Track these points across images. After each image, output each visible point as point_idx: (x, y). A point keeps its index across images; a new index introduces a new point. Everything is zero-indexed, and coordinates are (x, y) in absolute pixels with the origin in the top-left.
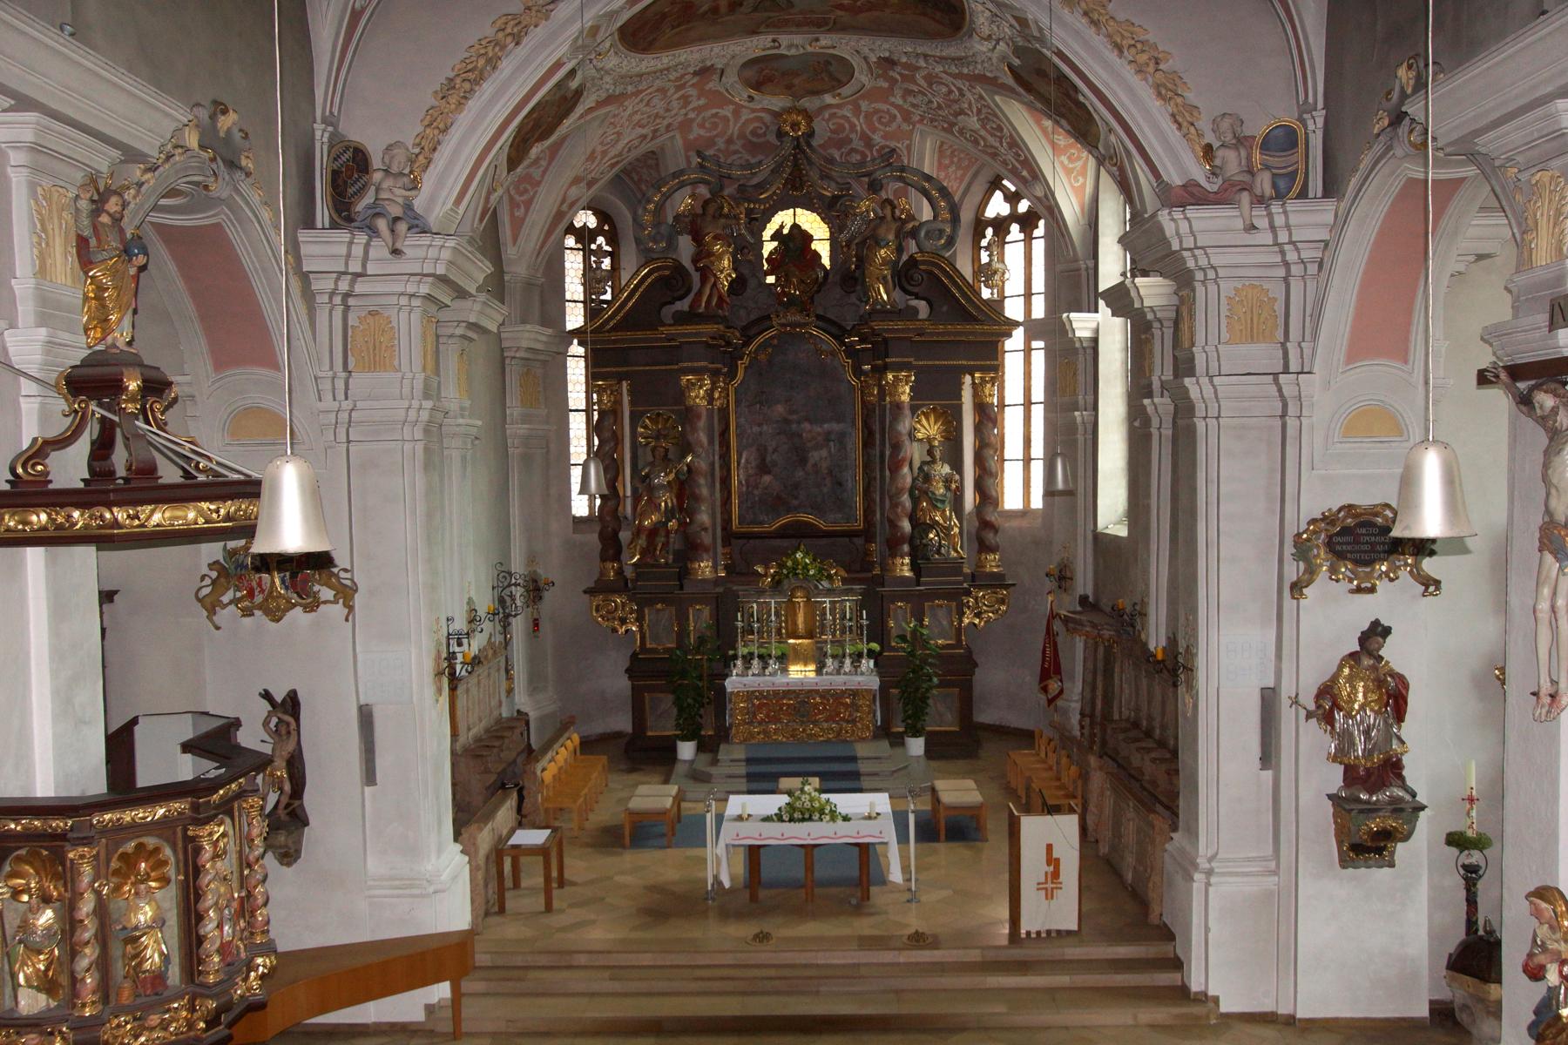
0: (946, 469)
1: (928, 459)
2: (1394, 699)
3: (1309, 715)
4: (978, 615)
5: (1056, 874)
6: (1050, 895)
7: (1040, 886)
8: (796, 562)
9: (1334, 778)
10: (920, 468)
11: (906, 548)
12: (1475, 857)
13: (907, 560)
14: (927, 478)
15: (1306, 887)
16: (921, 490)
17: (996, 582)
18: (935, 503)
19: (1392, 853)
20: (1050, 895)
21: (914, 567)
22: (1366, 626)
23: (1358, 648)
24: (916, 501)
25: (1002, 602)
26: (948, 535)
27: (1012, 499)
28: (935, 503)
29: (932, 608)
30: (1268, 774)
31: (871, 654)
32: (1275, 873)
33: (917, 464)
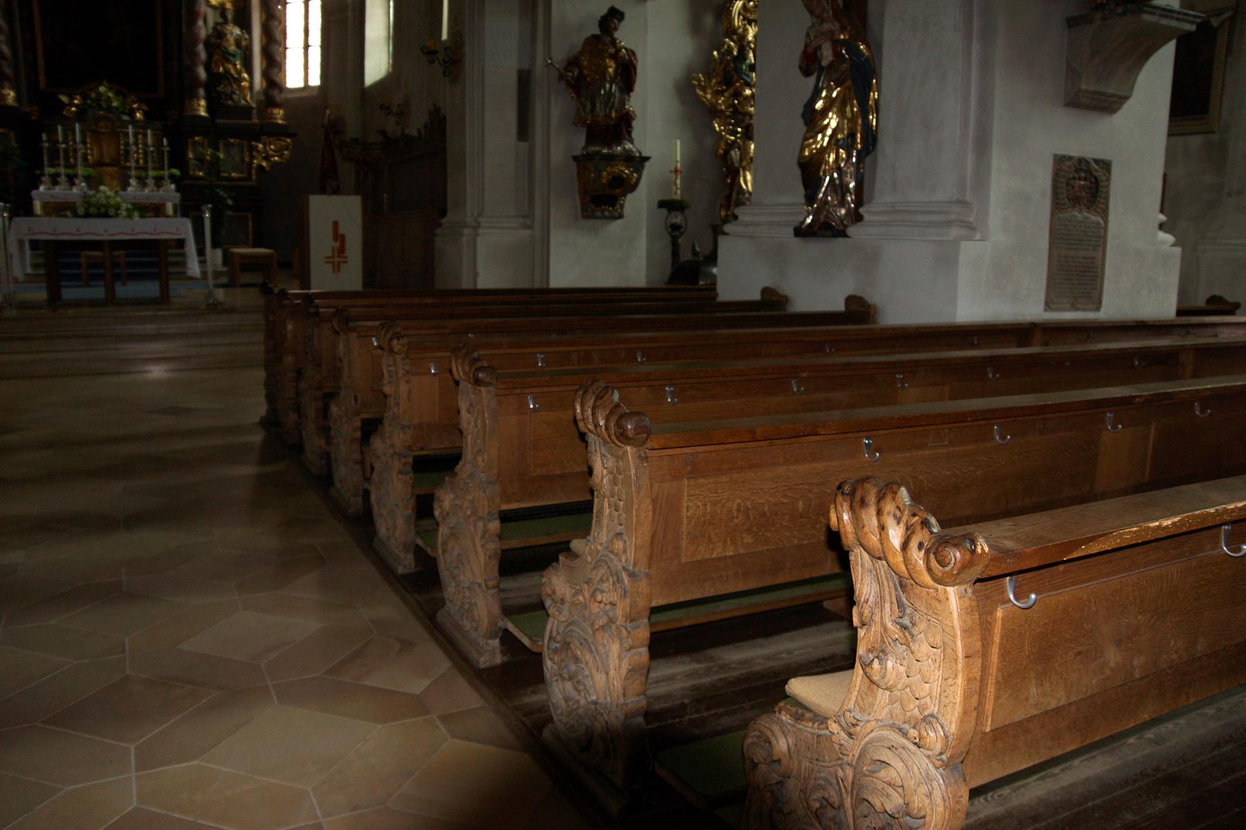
0: (237, 31)
1: (221, 20)
2: (627, 73)
3: (561, 77)
4: (267, 158)
5: (342, 250)
6: (337, 268)
7: (329, 260)
8: (99, 94)
9: (579, 142)
10: (215, 28)
11: (202, 92)
12: (678, 219)
13: (203, 103)
14: (219, 34)
15: (556, 237)
16: (216, 41)
17: (278, 132)
18: (227, 57)
19: (622, 206)
20: (337, 268)
21: (208, 109)
22: (604, 11)
23: (597, 31)
24: (210, 55)
25: (287, 148)
26: (239, 86)
27: (294, 78)
28: (227, 57)
29: (228, 145)
30: (524, 146)
31: (173, 178)
32: (530, 227)
33: (211, 23)
